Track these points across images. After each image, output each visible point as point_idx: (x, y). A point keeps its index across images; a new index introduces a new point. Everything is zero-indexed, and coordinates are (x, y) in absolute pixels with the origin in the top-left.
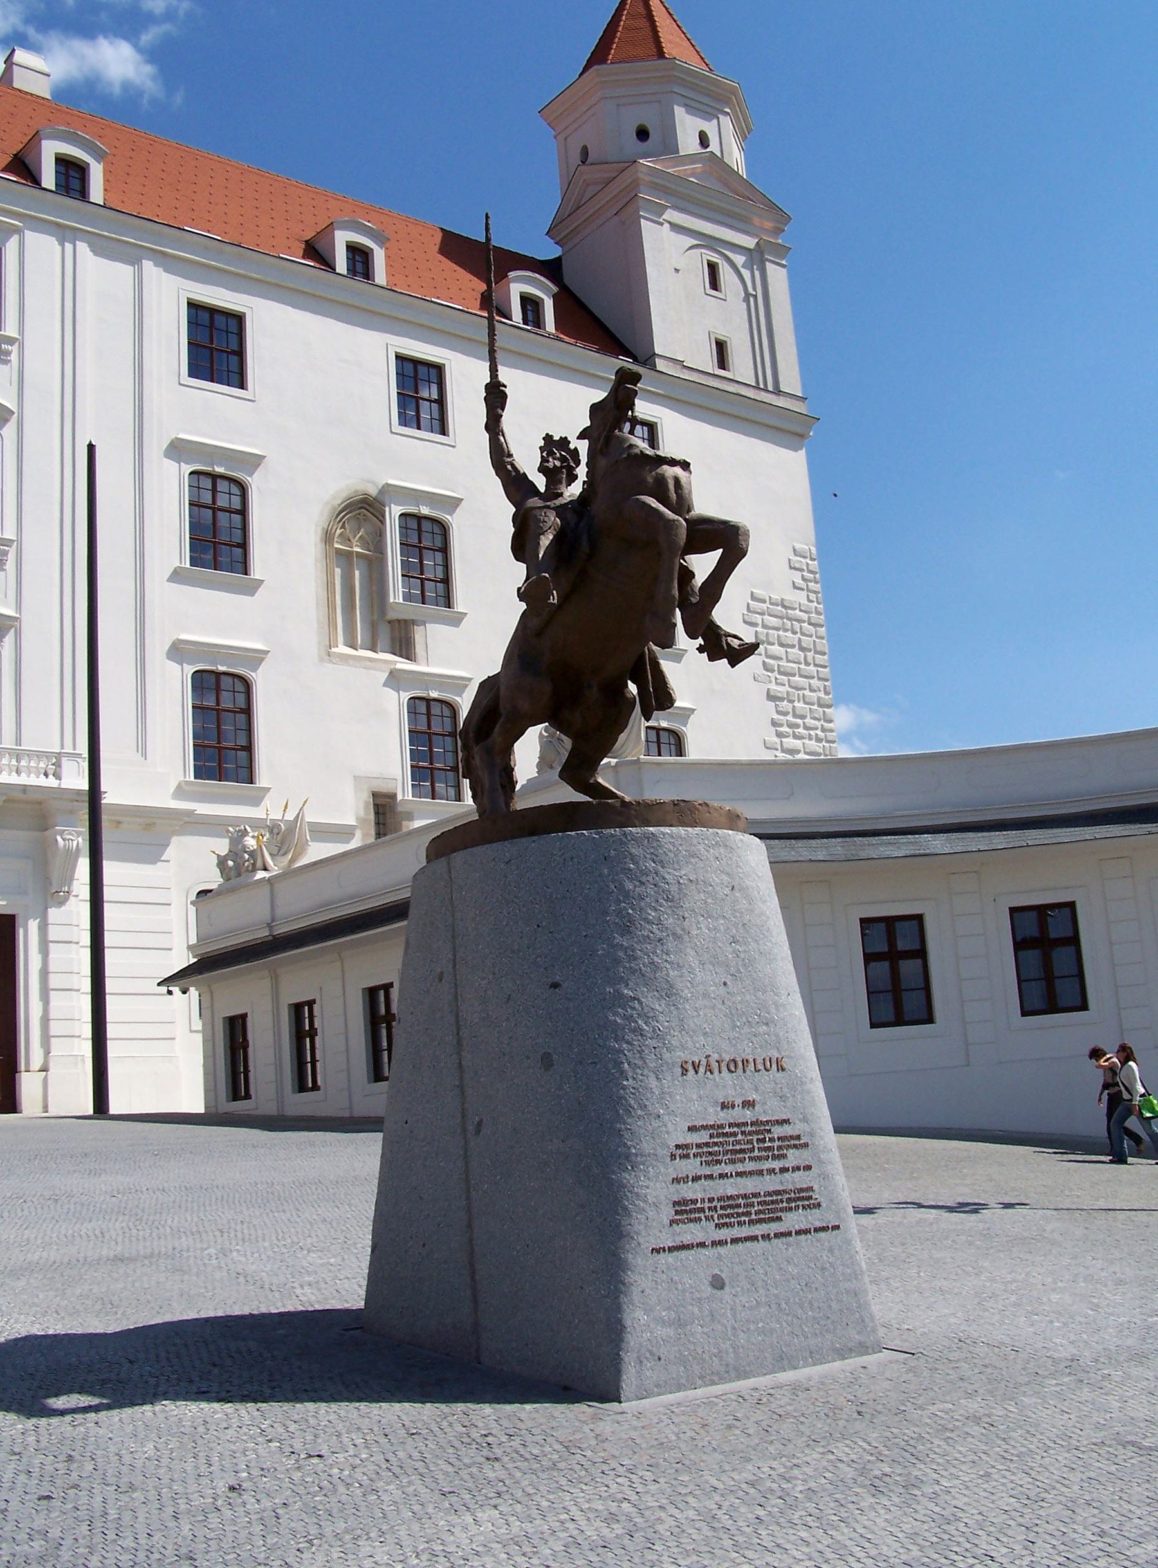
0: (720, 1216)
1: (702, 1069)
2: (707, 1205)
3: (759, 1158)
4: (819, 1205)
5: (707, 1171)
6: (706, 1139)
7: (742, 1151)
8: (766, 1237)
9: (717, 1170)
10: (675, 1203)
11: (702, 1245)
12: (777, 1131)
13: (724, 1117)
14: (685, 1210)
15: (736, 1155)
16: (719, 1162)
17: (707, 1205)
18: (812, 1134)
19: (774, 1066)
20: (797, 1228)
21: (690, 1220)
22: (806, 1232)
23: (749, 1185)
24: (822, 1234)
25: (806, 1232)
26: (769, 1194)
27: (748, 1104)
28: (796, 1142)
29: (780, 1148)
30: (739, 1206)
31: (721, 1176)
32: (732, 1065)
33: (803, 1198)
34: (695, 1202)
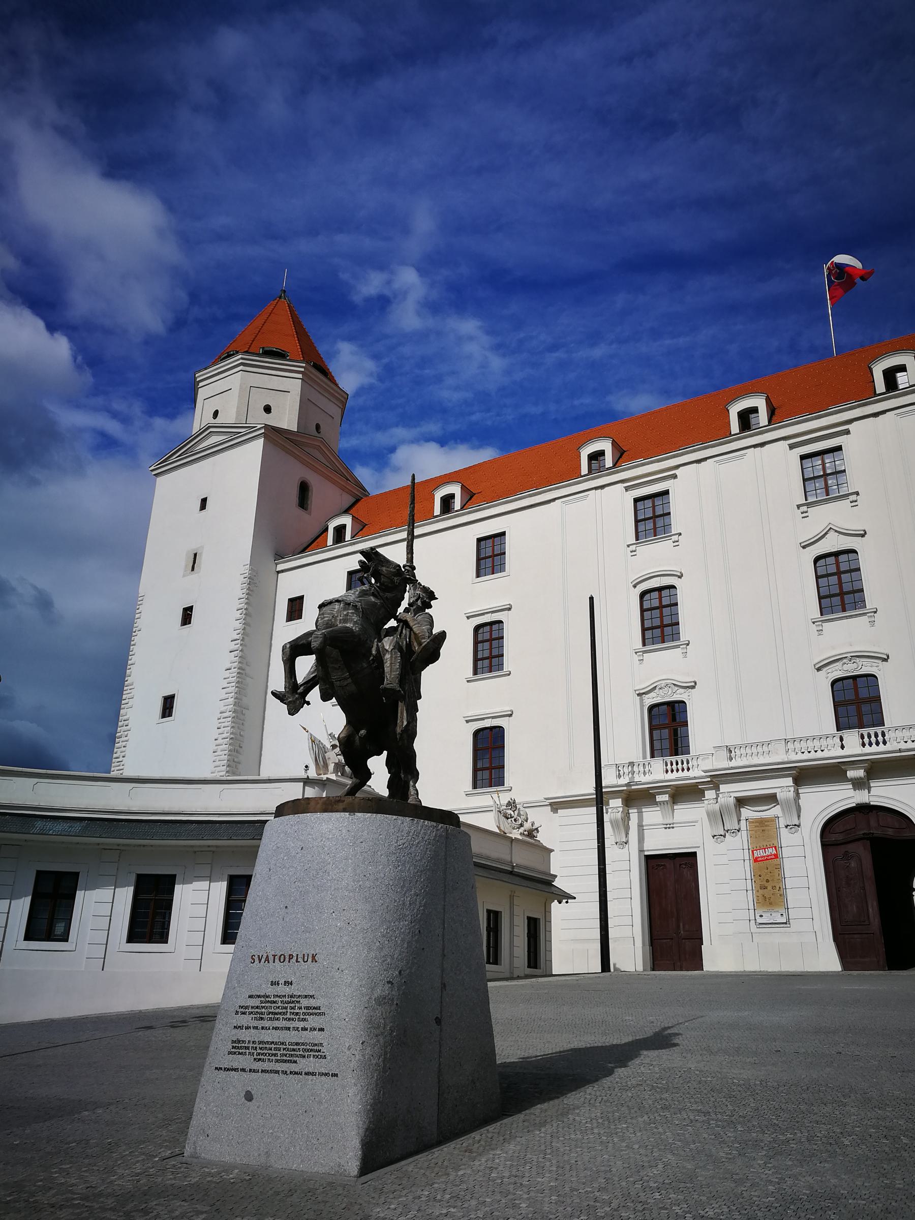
0: (259, 1054)
1: (263, 960)
2: (251, 1045)
3: (289, 1019)
4: (325, 1057)
5: (256, 1023)
6: (256, 1002)
7: (276, 1014)
8: (285, 1073)
9: (260, 1024)
10: (233, 1042)
11: (243, 1070)
12: (305, 1002)
13: (270, 991)
14: (238, 1047)
15: (274, 1016)
16: (262, 1019)
17: (251, 1045)
18: (330, 1007)
19: (310, 959)
20: (306, 1070)
21: (240, 1053)
22: (313, 1074)
23: (275, 1036)
24: (323, 1078)
25: (313, 1074)
26: (292, 1044)
27: (288, 983)
28: (315, 1011)
29: (304, 1014)
30: (271, 1049)
31: (263, 1028)
32: (282, 958)
33: (315, 1051)
34: (243, 1041)
